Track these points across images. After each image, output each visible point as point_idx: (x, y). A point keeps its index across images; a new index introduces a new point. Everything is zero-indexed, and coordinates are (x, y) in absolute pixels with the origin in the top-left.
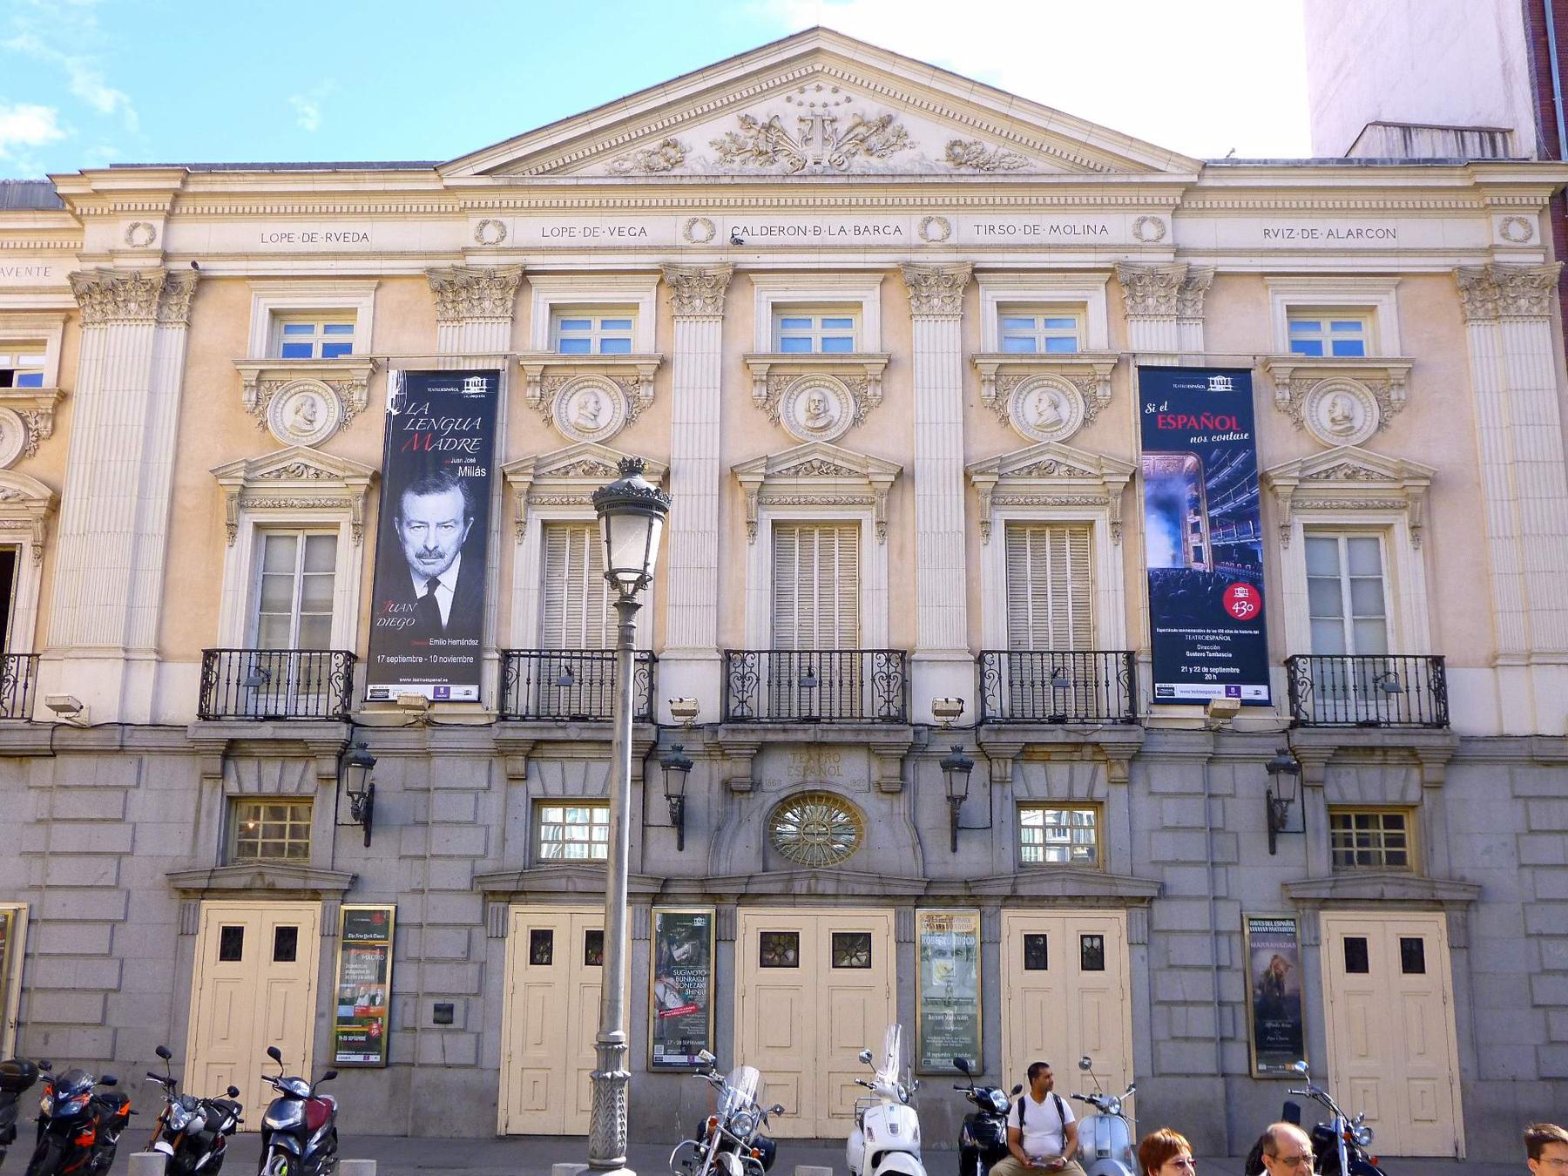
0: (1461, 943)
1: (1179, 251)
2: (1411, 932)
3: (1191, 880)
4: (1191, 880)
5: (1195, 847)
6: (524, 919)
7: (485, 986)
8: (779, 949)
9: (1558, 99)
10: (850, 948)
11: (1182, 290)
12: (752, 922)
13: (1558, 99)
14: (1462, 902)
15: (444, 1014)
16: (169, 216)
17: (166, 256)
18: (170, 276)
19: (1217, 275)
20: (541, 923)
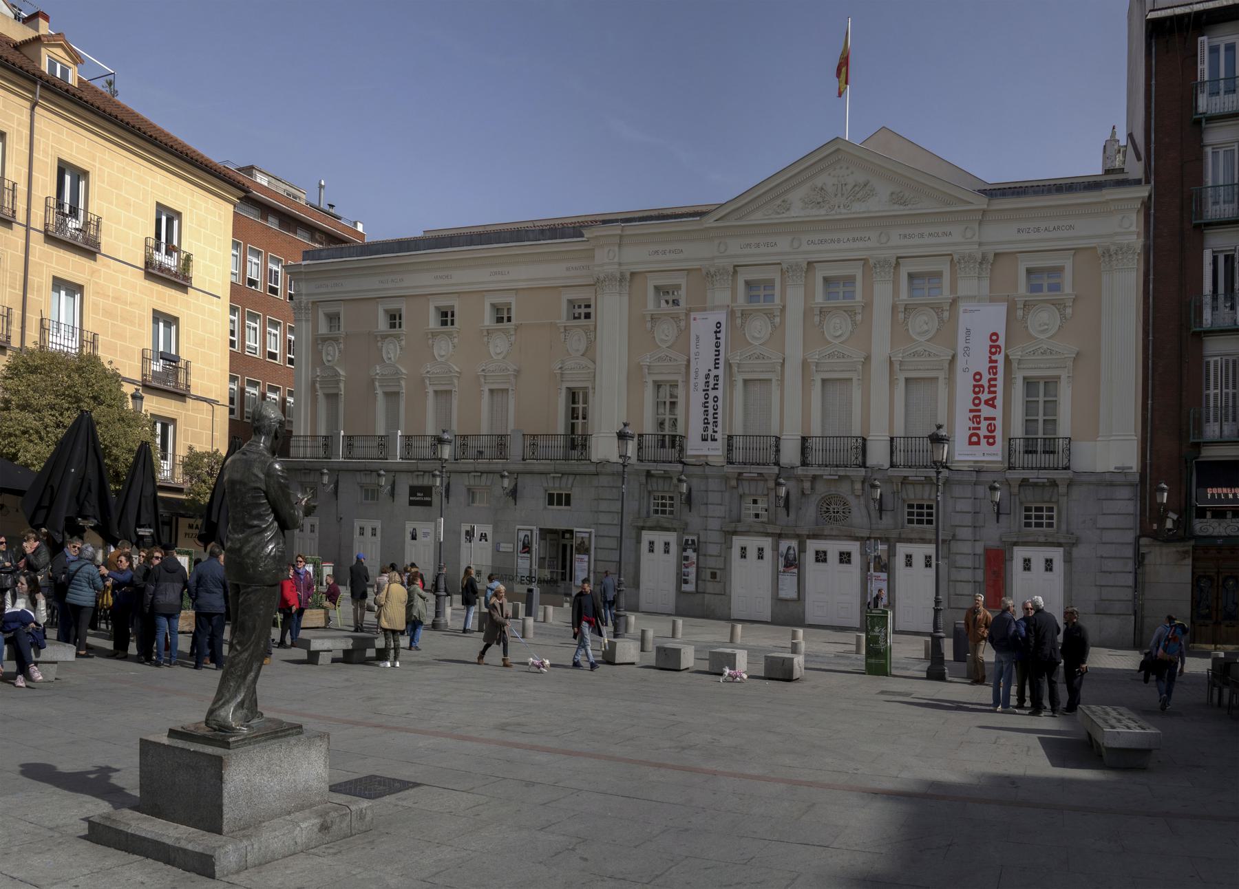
0: (1068, 560)
1: (980, 244)
2: (1049, 556)
3: (965, 533)
4: (965, 533)
5: (968, 520)
6: (738, 542)
7: (726, 568)
8: (821, 557)
9: (1153, 146)
10: (845, 558)
11: (981, 263)
12: (812, 546)
13: (1153, 146)
14: (1069, 545)
15: (714, 575)
16: (620, 245)
17: (620, 264)
18: (622, 275)
19: (996, 255)
20: (743, 544)
